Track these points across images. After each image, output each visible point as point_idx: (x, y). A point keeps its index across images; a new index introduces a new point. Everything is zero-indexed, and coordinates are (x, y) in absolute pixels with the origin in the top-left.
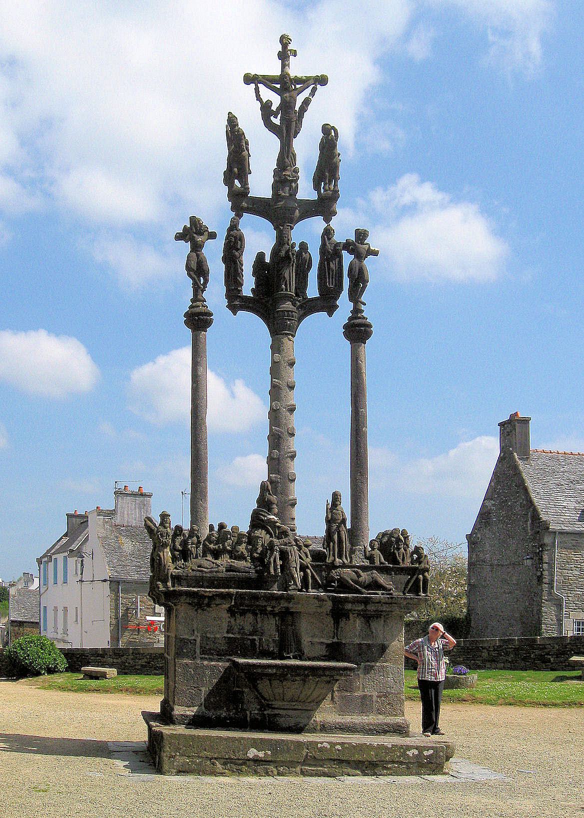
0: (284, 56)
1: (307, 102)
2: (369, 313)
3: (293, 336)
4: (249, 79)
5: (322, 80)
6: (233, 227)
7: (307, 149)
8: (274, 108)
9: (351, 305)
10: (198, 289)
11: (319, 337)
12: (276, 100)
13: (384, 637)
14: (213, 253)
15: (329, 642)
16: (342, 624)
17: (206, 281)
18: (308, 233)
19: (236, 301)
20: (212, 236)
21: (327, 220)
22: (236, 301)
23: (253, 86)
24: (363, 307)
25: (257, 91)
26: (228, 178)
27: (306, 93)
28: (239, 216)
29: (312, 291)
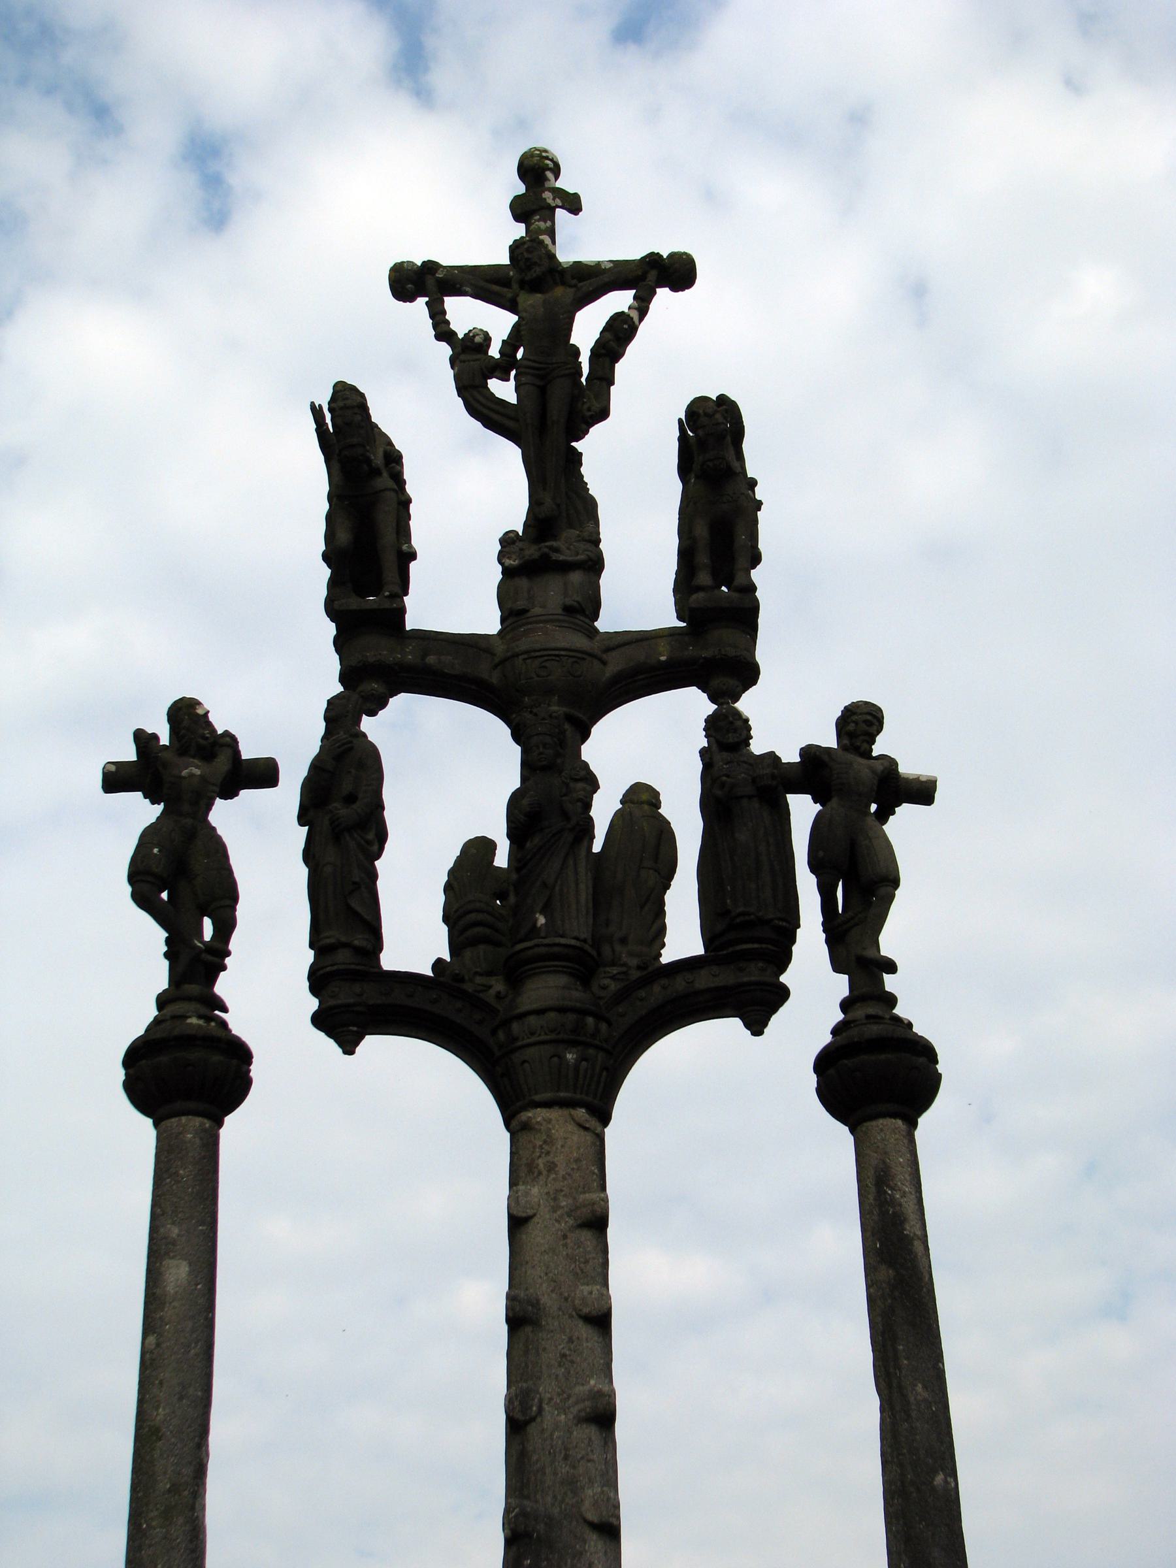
2: (916, 1001)
3: (605, 1118)
5: (677, 272)
6: (342, 718)
7: (631, 473)
8: (494, 351)
9: (841, 985)
10: (195, 968)
11: (717, 1120)
12: (497, 323)
17: (226, 927)
18: (647, 748)
19: (355, 996)
22: (355, 996)
23: (422, 301)
24: (890, 983)
25: (438, 316)
27: (620, 301)
29: (683, 936)
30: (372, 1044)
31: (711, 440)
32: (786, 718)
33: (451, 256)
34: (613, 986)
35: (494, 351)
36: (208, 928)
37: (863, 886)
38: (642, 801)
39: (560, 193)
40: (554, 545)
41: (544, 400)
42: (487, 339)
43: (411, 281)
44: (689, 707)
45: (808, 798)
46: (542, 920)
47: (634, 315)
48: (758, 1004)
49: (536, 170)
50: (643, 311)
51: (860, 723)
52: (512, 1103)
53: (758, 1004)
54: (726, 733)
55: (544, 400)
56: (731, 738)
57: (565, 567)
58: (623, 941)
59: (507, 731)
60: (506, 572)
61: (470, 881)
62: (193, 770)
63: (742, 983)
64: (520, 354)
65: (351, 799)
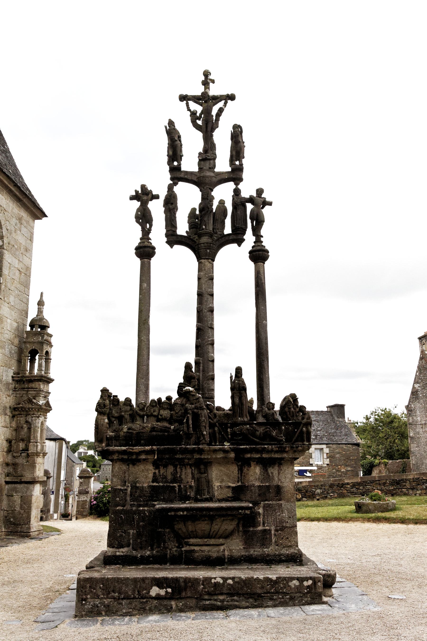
0: (206, 83)
1: (221, 111)
2: (266, 243)
3: (214, 261)
4: (183, 98)
5: (232, 97)
6: (170, 188)
8: (198, 115)
10: (146, 233)
11: (232, 261)
12: (198, 108)
13: (279, 480)
14: (157, 208)
15: (234, 485)
16: (245, 470)
17: (151, 226)
18: (223, 193)
19: (173, 239)
20: (157, 197)
21: (237, 184)
22: (173, 239)
23: (185, 102)
24: (262, 239)
26: (170, 162)
27: (221, 104)
28: (175, 184)
29: (228, 230)
30: (175, 247)
31: (237, 134)
32: (247, 190)
33: (190, 93)
34: (216, 238)
35: (198, 115)
36: (148, 226)
37: (258, 221)
38: (222, 202)
39: (210, 80)
40: (208, 155)
41: (207, 126)
42: (197, 112)
43: (183, 98)
44: (231, 186)
45: (250, 204)
46: (204, 227)
47: (224, 107)
48: (240, 242)
49: (206, 74)
50: (225, 106)
51: (260, 192)
52: (199, 258)
53: (240, 242)
54: (237, 192)
55: (207, 126)
56: (238, 194)
57: (210, 159)
58: (218, 229)
59: (199, 190)
60: (199, 160)
61: (192, 215)
62: (145, 198)
63: (237, 238)
64: (203, 116)
65: (172, 204)
